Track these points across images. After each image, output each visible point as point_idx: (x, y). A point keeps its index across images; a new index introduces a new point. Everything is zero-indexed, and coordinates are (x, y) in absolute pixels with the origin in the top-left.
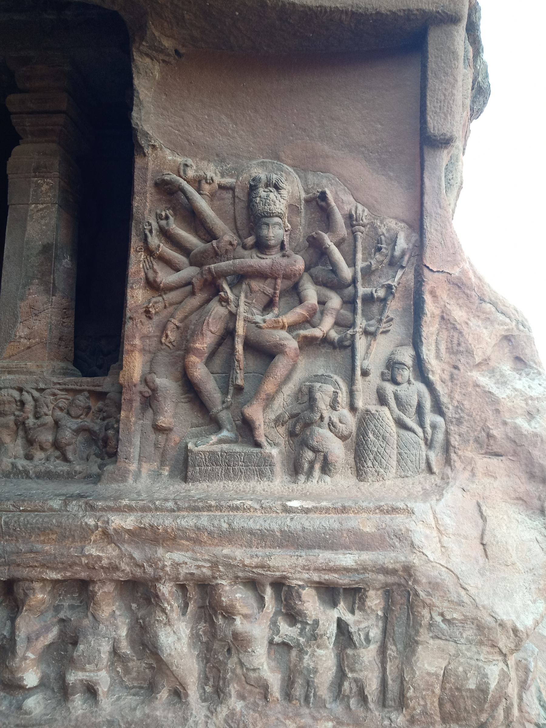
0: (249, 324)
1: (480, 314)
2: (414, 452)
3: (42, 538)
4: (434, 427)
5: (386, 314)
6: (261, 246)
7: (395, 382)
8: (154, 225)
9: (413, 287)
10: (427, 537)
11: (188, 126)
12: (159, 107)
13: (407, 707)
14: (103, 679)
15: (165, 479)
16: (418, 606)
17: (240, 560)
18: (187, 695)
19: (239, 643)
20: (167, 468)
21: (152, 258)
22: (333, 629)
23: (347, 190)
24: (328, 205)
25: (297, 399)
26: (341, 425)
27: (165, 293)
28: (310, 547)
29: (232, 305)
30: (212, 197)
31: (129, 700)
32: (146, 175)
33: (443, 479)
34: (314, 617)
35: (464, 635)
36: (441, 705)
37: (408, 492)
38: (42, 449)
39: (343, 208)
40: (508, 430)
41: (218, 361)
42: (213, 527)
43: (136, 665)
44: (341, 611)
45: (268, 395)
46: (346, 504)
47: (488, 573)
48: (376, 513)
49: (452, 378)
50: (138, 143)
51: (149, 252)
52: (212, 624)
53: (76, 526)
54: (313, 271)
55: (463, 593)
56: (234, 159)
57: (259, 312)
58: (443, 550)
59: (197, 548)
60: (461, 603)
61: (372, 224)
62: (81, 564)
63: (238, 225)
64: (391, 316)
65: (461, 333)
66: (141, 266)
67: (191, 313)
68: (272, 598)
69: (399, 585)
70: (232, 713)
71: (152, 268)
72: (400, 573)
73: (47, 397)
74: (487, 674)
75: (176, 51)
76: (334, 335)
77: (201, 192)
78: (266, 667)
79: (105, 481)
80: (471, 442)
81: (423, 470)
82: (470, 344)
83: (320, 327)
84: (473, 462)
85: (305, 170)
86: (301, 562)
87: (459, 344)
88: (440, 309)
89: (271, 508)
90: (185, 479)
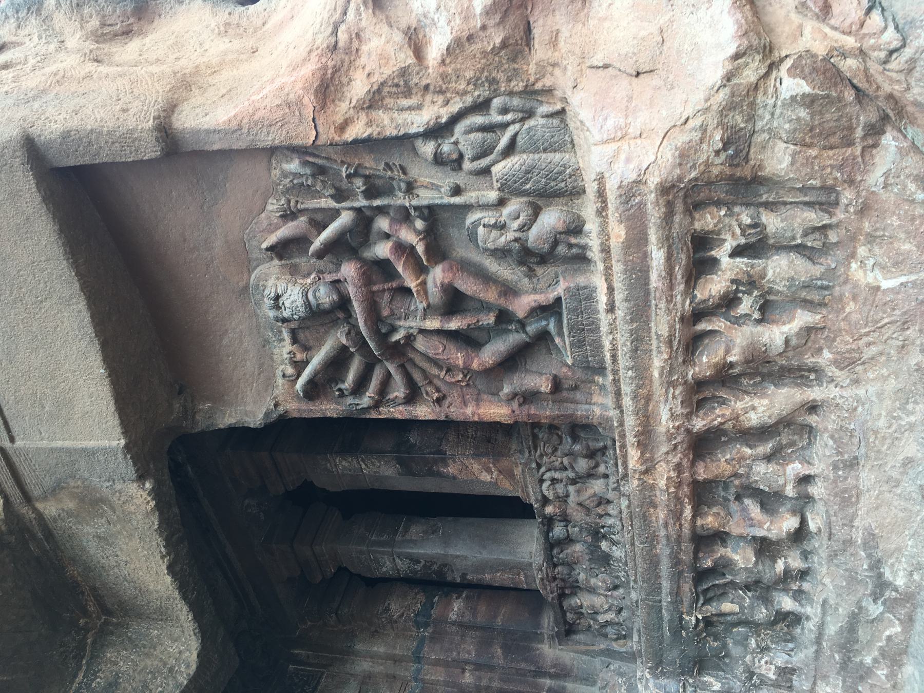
1: (354, 49)
4: (504, 111)
5: (382, 173)
8: (350, 400)
10: (628, 160)
11: (245, 374)
14: (795, 468)
16: (709, 178)
18: (814, 401)
20: (596, 378)
22: (741, 262)
24: (278, 243)
26: (521, 218)
28: (647, 293)
32: (304, 410)
34: (729, 284)
35: (743, 125)
36: (831, 148)
39: (277, 224)
40: (491, 23)
44: (722, 254)
45: (500, 297)
48: (607, 215)
49: (441, 92)
51: (377, 405)
55: (691, 124)
59: (656, 397)
60: (703, 129)
62: (676, 492)
65: (382, 84)
66: (392, 410)
68: (710, 321)
69: (686, 196)
70: (835, 363)
74: (792, 96)
75: (180, 393)
78: (786, 328)
80: (516, 66)
81: (561, 121)
84: (541, 63)
86: (663, 305)
87: (397, 85)
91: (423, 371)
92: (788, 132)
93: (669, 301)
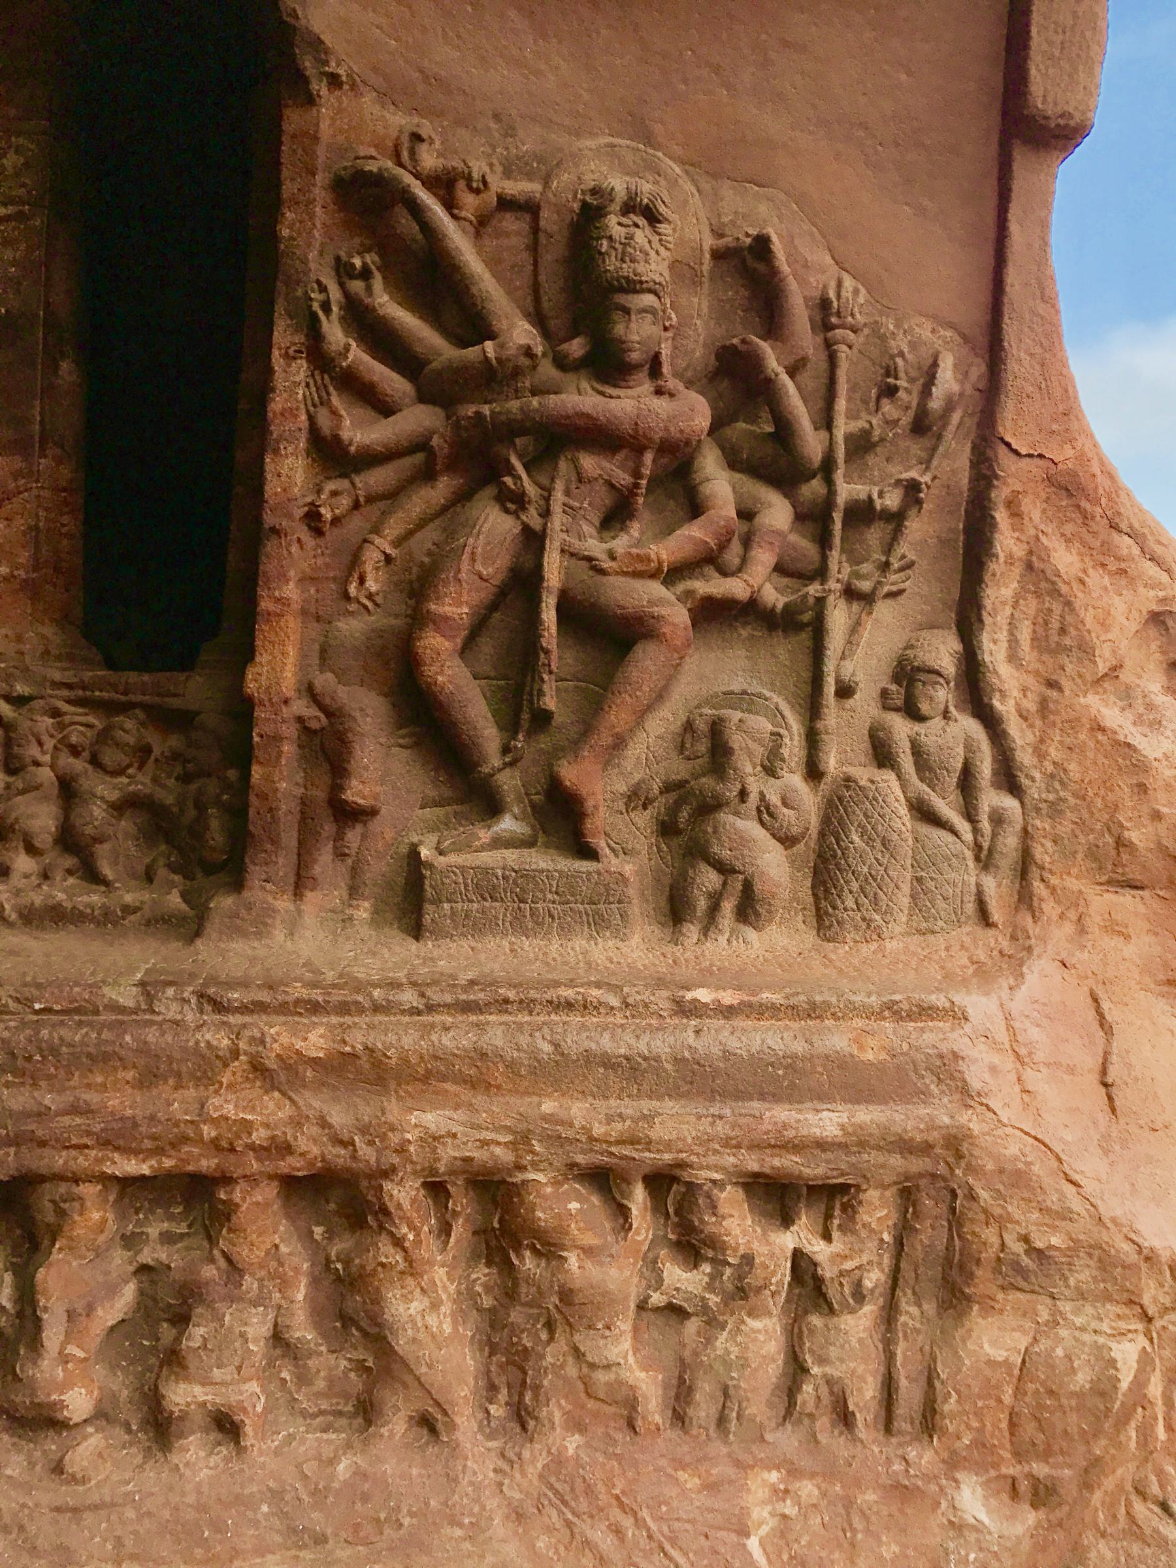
0: (573, 560)
3: (99, 1079)
7: (913, 712)
8: (335, 294)
9: (965, 488)
10: (993, 1069)
11: (424, 30)
13: (944, 1432)
14: (250, 1396)
15: (365, 931)
17: (583, 1128)
18: (452, 1427)
19: (569, 1310)
23: (817, 234)
24: (774, 272)
25: (681, 748)
26: (785, 810)
27: (358, 471)
28: (740, 1095)
30: (481, 225)
31: (312, 1441)
32: (312, 155)
33: (1014, 938)
34: (741, 1251)
35: (1072, 1282)
36: (1012, 1425)
37: (943, 968)
40: (1163, 832)
41: (487, 646)
42: (518, 1050)
43: (330, 1364)
44: (801, 1235)
47: (1117, 1148)
48: (884, 1019)
52: (508, 1268)
53: (184, 1049)
54: (728, 431)
55: (1070, 1189)
57: (593, 531)
58: (1026, 1097)
59: (480, 1100)
60: (1066, 1215)
61: (875, 327)
62: (200, 1140)
63: (546, 305)
64: (912, 556)
65: (1068, 603)
66: (300, 397)
67: (422, 523)
68: (645, 1209)
69: (934, 1176)
70: (558, 1461)
71: (325, 402)
72: (938, 1150)
73: (39, 718)
74: (1115, 1361)
76: (774, 596)
77: (456, 211)
79: (214, 936)
80: (1080, 856)
81: (968, 917)
82: (1089, 632)
83: (746, 577)
84: (1082, 902)
85: (715, 176)
86: (721, 1128)
87: (1063, 631)
88: (1026, 546)
89: (646, 1006)
90: (416, 931)
91: (393, 495)
92: (1050, 1353)
93: (727, 1143)
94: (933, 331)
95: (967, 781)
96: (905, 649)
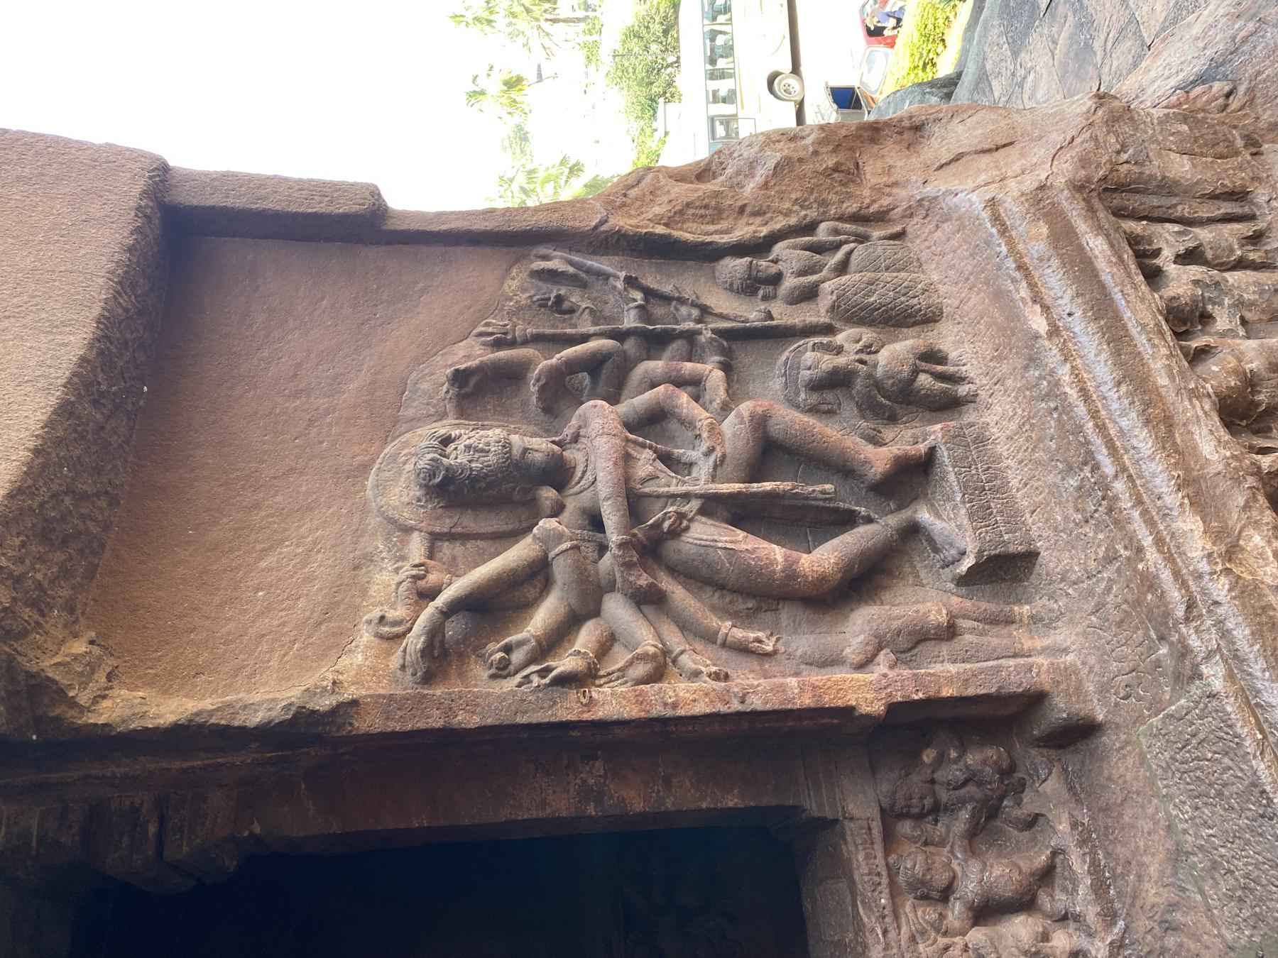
2: (880, 250)
6: (557, 473)
7: (777, 279)
11: (284, 624)
12: (231, 685)
20: (1016, 608)
21: (602, 673)
25: (831, 413)
29: (687, 508)
33: (911, 215)
38: (1045, 937)
46: (1014, 266)
50: (325, 714)
55: (1078, 140)
56: (366, 538)
59: (1180, 419)
61: (511, 314)
63: (511, 527)
65: (688, 205)
87: (706, 207)
90: (1030, 557)
94: (513, 279)
95: (818, 249)
96: (732, 290)
